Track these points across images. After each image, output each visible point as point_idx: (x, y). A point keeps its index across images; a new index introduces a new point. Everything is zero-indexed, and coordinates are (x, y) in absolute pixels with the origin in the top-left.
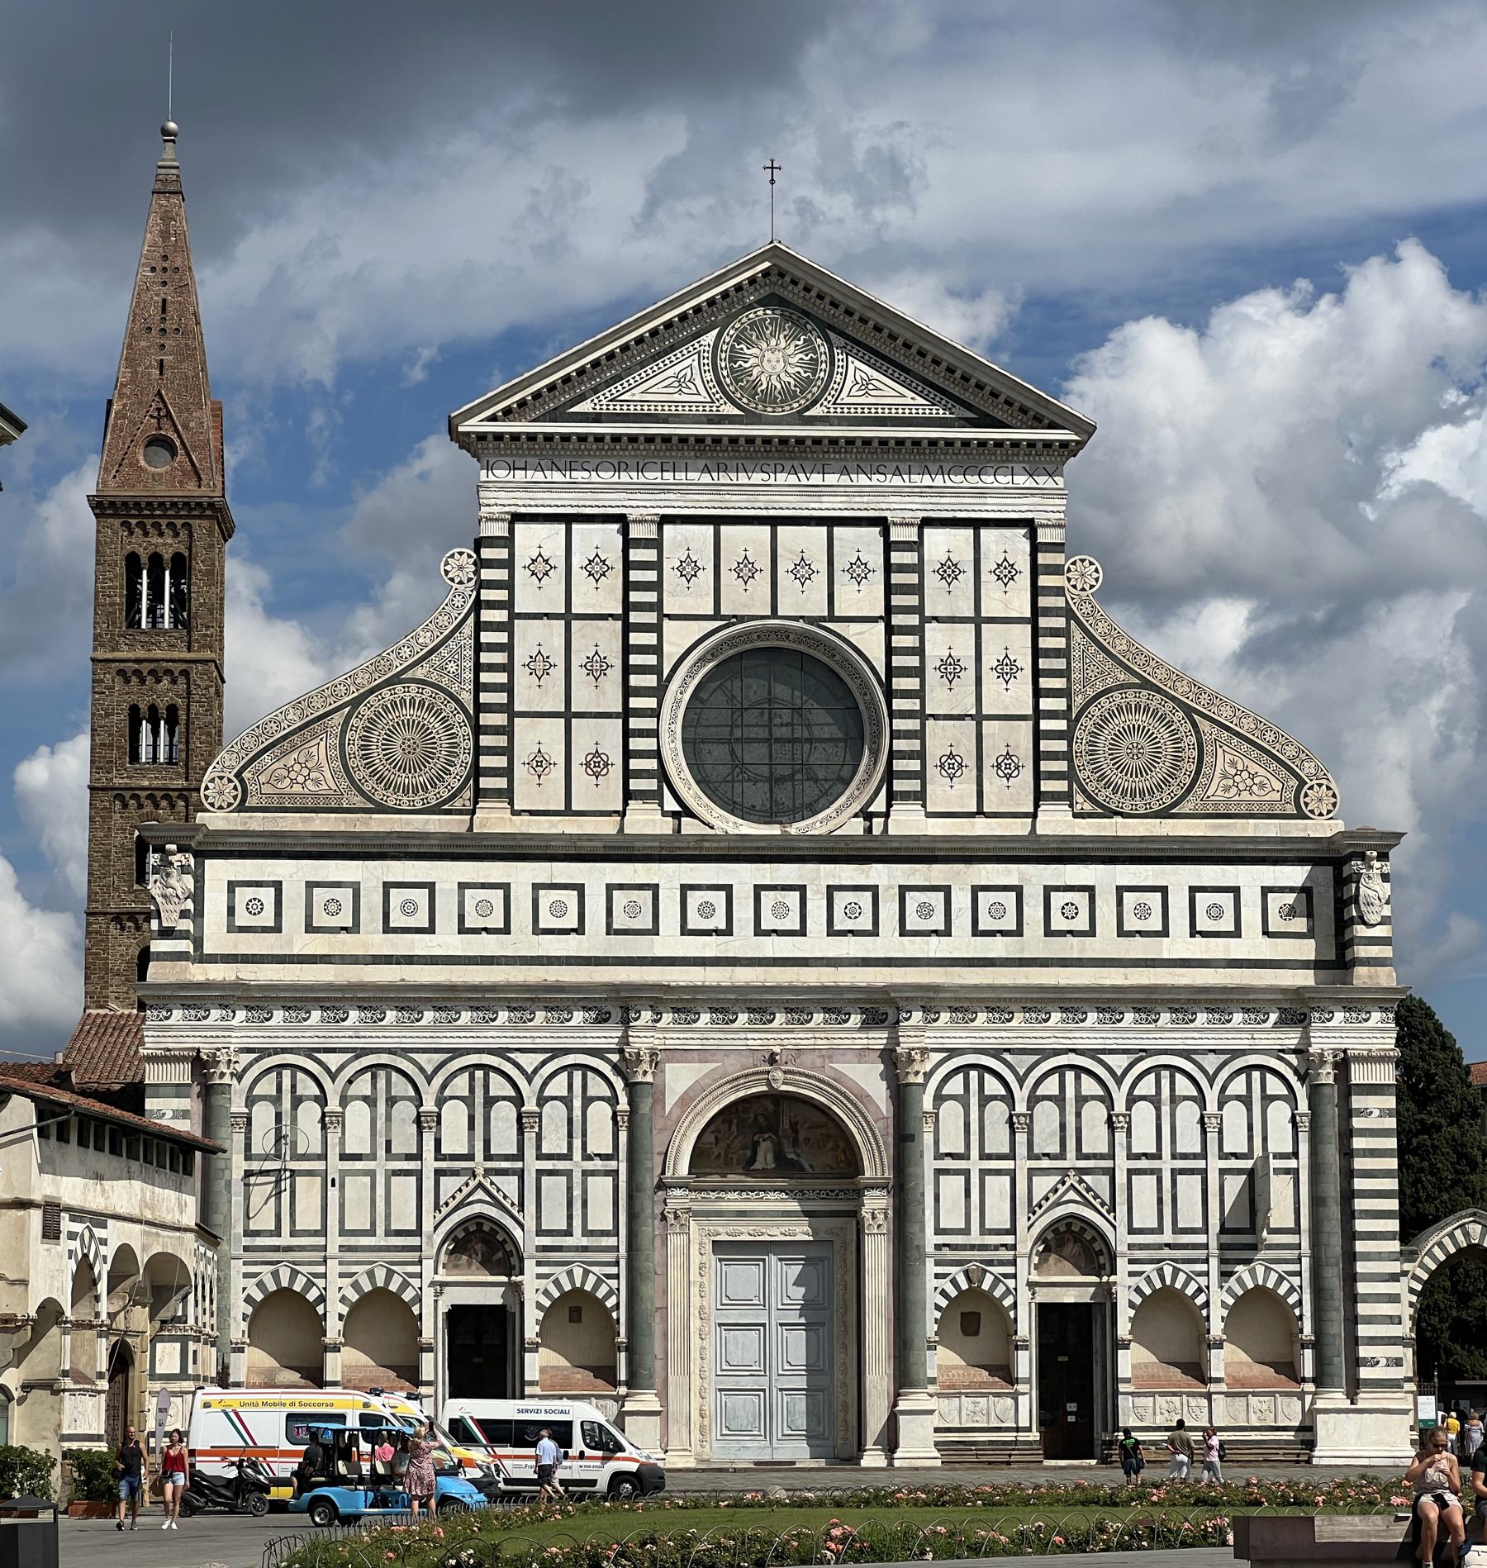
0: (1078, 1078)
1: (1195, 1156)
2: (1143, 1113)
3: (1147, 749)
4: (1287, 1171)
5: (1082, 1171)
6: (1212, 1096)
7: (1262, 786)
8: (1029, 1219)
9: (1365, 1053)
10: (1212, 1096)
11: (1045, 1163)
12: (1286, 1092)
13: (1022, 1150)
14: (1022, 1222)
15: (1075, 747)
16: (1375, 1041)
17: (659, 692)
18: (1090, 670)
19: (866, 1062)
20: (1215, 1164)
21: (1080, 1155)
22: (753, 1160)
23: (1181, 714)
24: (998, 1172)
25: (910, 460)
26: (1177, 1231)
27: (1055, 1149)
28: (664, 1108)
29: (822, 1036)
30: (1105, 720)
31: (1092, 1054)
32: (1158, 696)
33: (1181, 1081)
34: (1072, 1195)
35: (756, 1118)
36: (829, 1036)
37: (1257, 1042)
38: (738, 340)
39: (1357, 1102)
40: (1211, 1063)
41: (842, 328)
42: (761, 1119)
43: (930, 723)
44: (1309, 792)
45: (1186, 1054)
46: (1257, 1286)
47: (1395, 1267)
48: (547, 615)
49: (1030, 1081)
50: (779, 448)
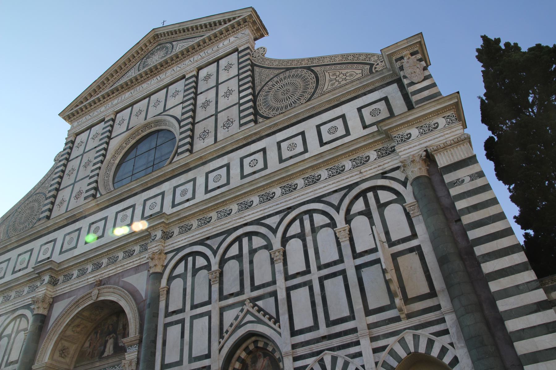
0: (250, 240)
1: (335, 263)
2: (295, 246)
3: (291, 89)
4: (411, 250)
5: (254, 300)
6: (340, 218)
7: (351, 75)
8: (220, 342)
9: (442, 146)
10: (340, 218)
11: (231, 301)
12: (395, 197)
13: (215, 295)
14: (215, 346)
15: (257, 103)
16: (447, 136)
17: (102, 162)
18: (261, 76)
19: (139, 272)
20: (349, 265)
21: (254, 288)
22: (104, 351)
23: (305, 70)
24: (201, 315)
25: (194, 56)
26: (330, 323)
27: (237, 289)
28: (47, 328)
29: (120, 265)
30: (270, 89)
31: (257, 222)
32: (294, 70)
33: (316, 216)
34: (249, 318)
35: (108, 328)
36: (122, 264)
37: (364, 174)
38: (146, 59)
39: (448, 178)
40: (335, 199)
41: (177, 40)
42: (111, 327)
43: (196, 126)
44: (377, 66)
45: (318, 200)
46: (409, 353)
47: (539, 295)
48: (77, 157)
49: (221, 251)
50: (151, 74)
